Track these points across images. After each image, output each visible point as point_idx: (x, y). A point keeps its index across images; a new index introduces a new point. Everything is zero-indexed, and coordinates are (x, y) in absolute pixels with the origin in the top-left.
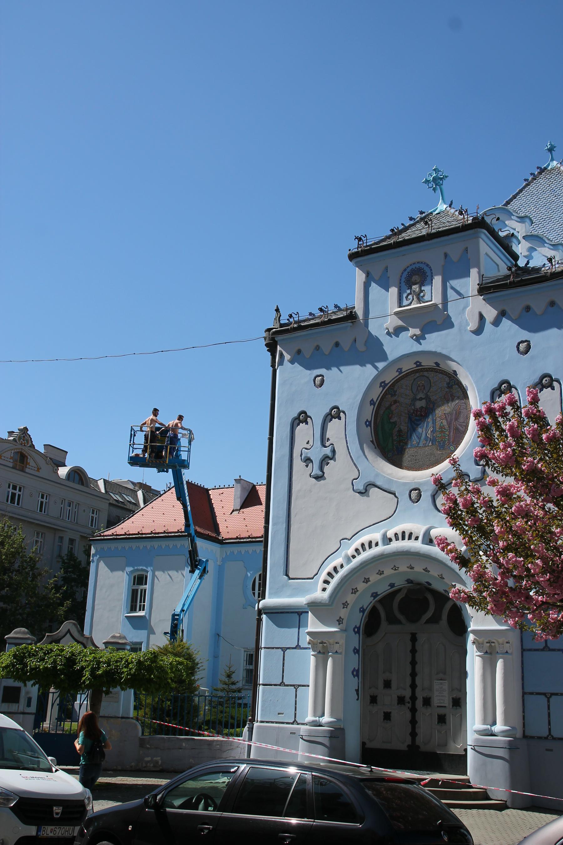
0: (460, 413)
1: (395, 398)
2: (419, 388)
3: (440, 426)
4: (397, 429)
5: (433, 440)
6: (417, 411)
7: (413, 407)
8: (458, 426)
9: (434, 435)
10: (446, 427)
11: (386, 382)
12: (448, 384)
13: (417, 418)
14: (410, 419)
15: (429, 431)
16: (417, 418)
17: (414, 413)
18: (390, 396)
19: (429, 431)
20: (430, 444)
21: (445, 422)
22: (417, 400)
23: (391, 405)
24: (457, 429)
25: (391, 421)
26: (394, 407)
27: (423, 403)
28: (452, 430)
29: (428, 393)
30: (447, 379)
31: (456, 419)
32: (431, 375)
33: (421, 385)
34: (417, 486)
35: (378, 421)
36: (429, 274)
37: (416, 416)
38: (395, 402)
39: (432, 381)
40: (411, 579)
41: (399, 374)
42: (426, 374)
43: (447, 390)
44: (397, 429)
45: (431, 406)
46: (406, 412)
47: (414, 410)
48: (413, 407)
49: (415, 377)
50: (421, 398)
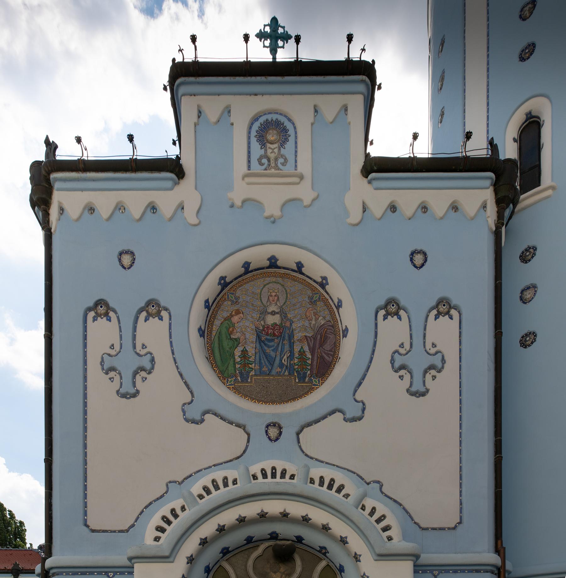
0: (326, 338)
2: (271, 298)
3: (300, 351)
4: (240, 348)
5: (290, 369)
8: (323, 354)
12: (311, 298)
13: (268, 337)
14: (259, 337)
15: (285, 357)
16: (268, 337)
17: (263, 330)
18: (230, 303)
19: (285, 357)
20: (287, 373)
21: (306, 348)
22: (269, 313)
23: (231, 316)
24: (322, 357)
25: (233, 337)
26: (235, 319)
28: (316, 358)
30: (309, 293)
31: (321, 345)
32: (289, 283)
33: (274, 294)
35: (214, 333)
38: (238, 312)
39: (288, 291)
42: (280, 280)
43: (310, 306)
44: (240, 348)
45: (288, 324)
46: (254, 327)
47: (263, 326)
48: (262, 323)
49: (266, 282)
50: (274, 311)
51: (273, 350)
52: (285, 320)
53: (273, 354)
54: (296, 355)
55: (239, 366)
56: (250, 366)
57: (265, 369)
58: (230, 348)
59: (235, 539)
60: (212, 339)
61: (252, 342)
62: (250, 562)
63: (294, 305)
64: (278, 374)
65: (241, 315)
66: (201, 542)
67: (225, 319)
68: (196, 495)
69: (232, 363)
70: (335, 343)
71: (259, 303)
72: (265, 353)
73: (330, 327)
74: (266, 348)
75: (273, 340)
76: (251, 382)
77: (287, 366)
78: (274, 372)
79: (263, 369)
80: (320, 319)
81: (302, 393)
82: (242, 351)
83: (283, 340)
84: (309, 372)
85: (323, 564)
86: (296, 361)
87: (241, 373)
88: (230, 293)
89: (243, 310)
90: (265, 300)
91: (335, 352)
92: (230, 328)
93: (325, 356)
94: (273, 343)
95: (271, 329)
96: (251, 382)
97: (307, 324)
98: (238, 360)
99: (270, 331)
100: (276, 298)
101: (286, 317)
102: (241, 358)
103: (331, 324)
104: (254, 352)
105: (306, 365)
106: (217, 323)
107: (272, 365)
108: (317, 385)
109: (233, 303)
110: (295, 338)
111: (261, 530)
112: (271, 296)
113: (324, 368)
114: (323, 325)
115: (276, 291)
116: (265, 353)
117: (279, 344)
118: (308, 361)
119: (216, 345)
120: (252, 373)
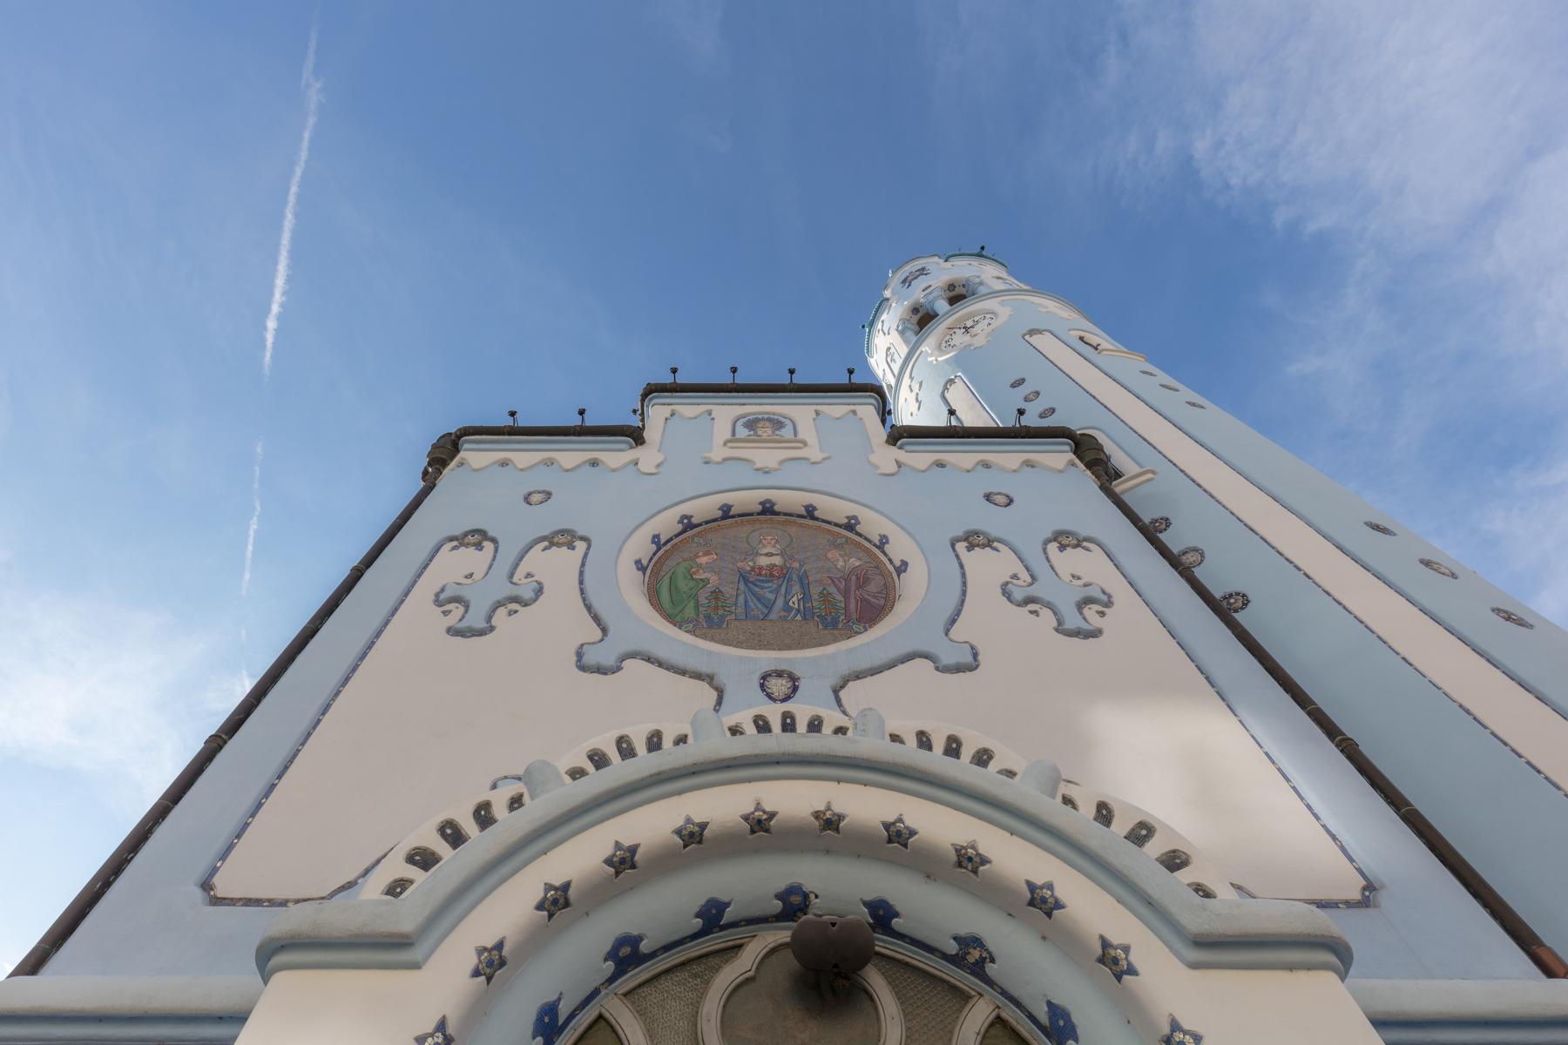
5: (807, 615)
6: (761, 568)
11: (694, 521)
20: (799, 617)
24: (863, 600)
27: (777, 560)
28: (853, 601)
31: (859, 587)
36: (787, 422)
40: (807, 888)
47: (753, 569)
53: (771, 596)
54: (815, 597)
59: (658, 911)
62: (712, 1006)
64: (783, 619)
66: (545, 899)
68: (562, 771)
69: (692, 603)
78: (773, 616)
85: (978, 1015)
87: (708, 618)
91: (887, 595)
98: (703, 601)
101: (791, 557)
107: (770, 609)
111: (749, 882)
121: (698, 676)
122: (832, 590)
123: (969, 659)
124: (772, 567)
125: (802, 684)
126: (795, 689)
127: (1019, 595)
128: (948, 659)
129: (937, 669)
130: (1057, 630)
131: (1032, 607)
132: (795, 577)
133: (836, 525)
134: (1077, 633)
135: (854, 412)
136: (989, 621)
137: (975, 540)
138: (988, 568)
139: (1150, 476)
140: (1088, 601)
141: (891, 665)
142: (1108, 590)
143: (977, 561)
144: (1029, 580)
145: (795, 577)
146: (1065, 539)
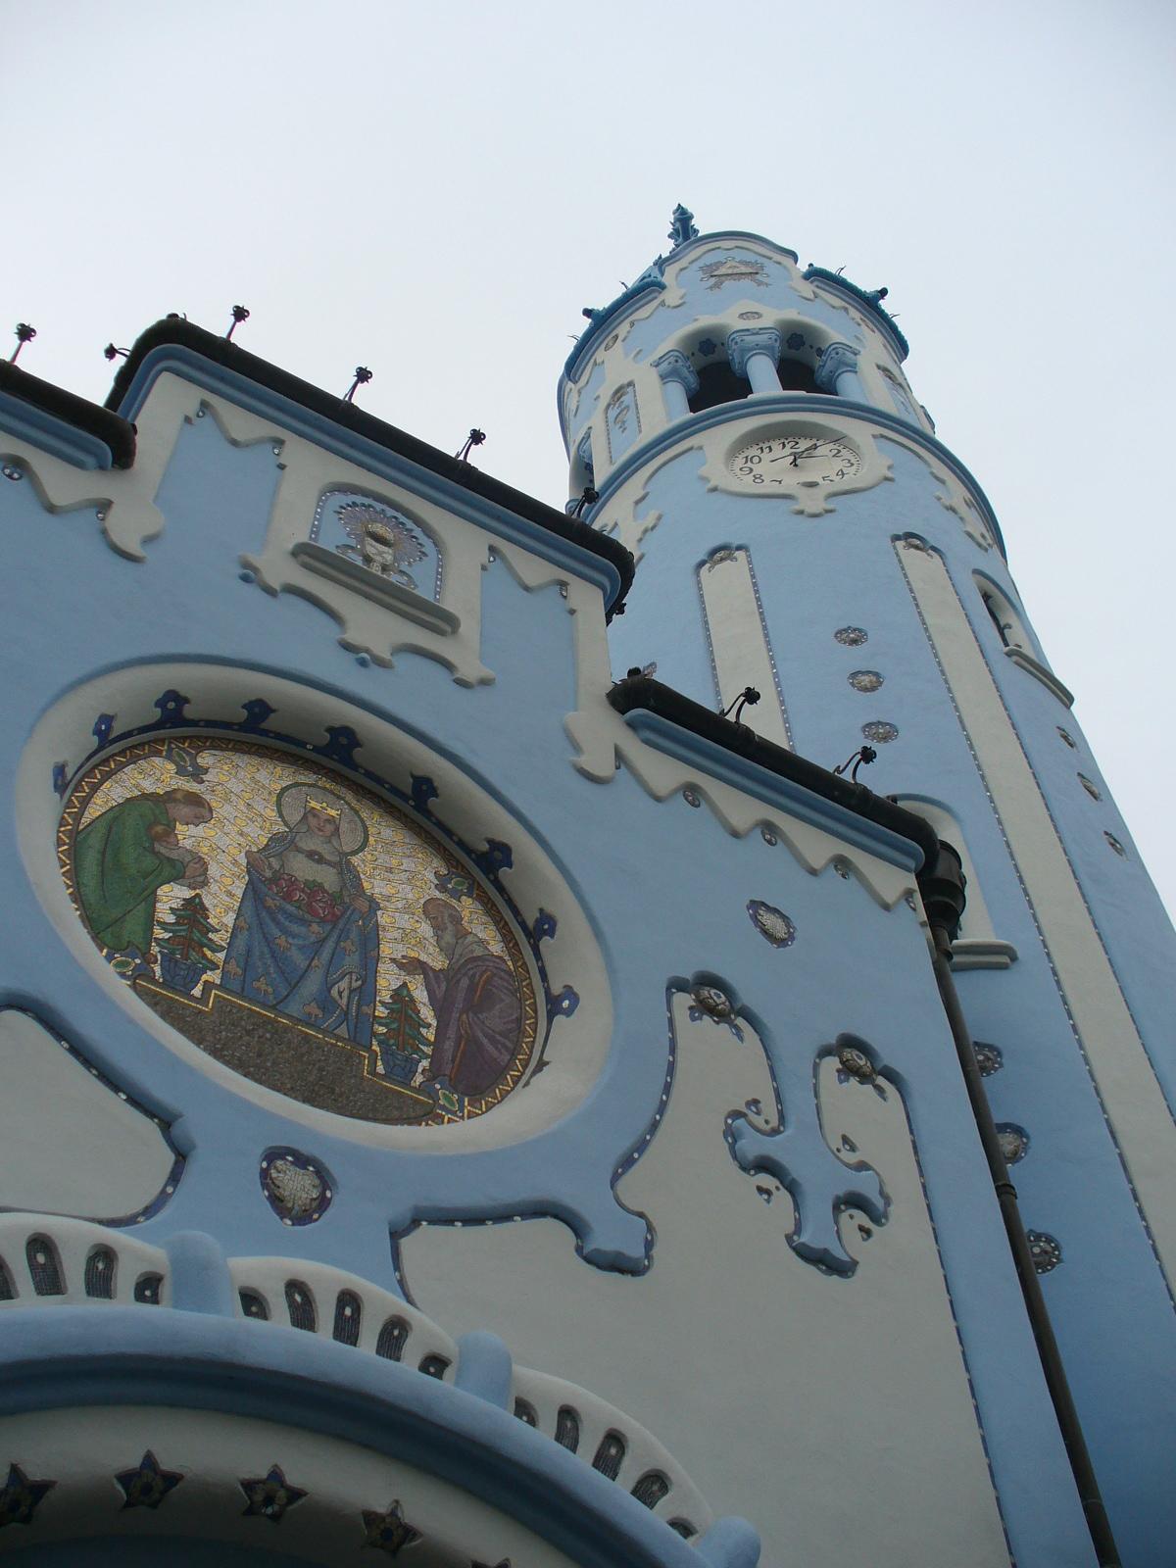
1: (193, 787)
2: (313, 821)
6: (293, 882)
7: (275, 863)
9: (365, 1009)
10: (427, 1014)
11: (189, 712)
13: (290, 908)
14: (254, 891)
16: (290, 908)
19: (344, 984)
20: (343, 1031)
21: (420, 994)
22: (299, 850)
25: (158, 847)
27: (328, 878)
28: (451, 1033)
29: (355, 860)
34: (306, 1149)
37: (287, 897)
39: (371, 830)
41: (243, 727)
42: (349, 796)
43: (438, 894)
46: (244, 861)
49: (302, 779)
51: (301, 948)
52: (353, 891)
53: (299, 959)
55: (167, 935)
56: (208, 953)
57: (262, 984)
58: (146, 875)
60: (85, 820)
61: (230, 894)
63: (390, 870)
65: (205, 812)
67: (145, 796)
70: (519, 1021)
71: (271, 813)
72: (268, 940)
73: (502, 974)
74: (276, 932)
75: (307, 923)
76: (204, 999)
77: (346, 1013)
78: (294, 1008)
79: (256, 984)
80: (470, 938)
81: (396, 1113)
82: (188, 902)
83: (343, 935)
84: (425, 1063)
86: (381, 1012)
87: (168, 961)
88: (178, 747)
89: (213, 804)
90: (295, 817)
92: (157, 822)
93: (485, 1041)
94: (303, 929)
95: (303, 891)
96: (204, 999)
97: (426, 929)
99: (297, 895)
100: (329, 828)
102: (178, 917)
103: (504, 967)
104: (229, 919)
105: (414, 1038)
106: (114, 792)
107: (293, 987)
108: (454, 1113)
109: (181, 771)
110: (386, 950)
112: (315, 816)
113: (480, 1072)
114: (478, 958)
115: (333, 813)
116: (268, 940)
117: (324, 940)
118: (424, 1031)
119: (95, 841)
120: (213, 976)
121: (140, 1102)
122: (420, 994)
123: (636, 1251)
124: (314, 889)
125: (340, 1201)
126: (323, 1204)
127: (753, 1146)
128: (603, 1240)
129: (579, 1250)
130: (789, 1238)
131: (767, 1180)
132: (354, 934)
133: (461, 844)
134: (812, 1256)
135: (563, 584)
136: (693, 1191)
137: (712, 997)
138: (719, 1065)
139: (1005, 959)
140: (854, 1201)
141: (503, 1216)
142: (889, 1190)
143: (703, 1037)
144: (774, 1122)
145: (354, 934)
146: (856, 1058)
